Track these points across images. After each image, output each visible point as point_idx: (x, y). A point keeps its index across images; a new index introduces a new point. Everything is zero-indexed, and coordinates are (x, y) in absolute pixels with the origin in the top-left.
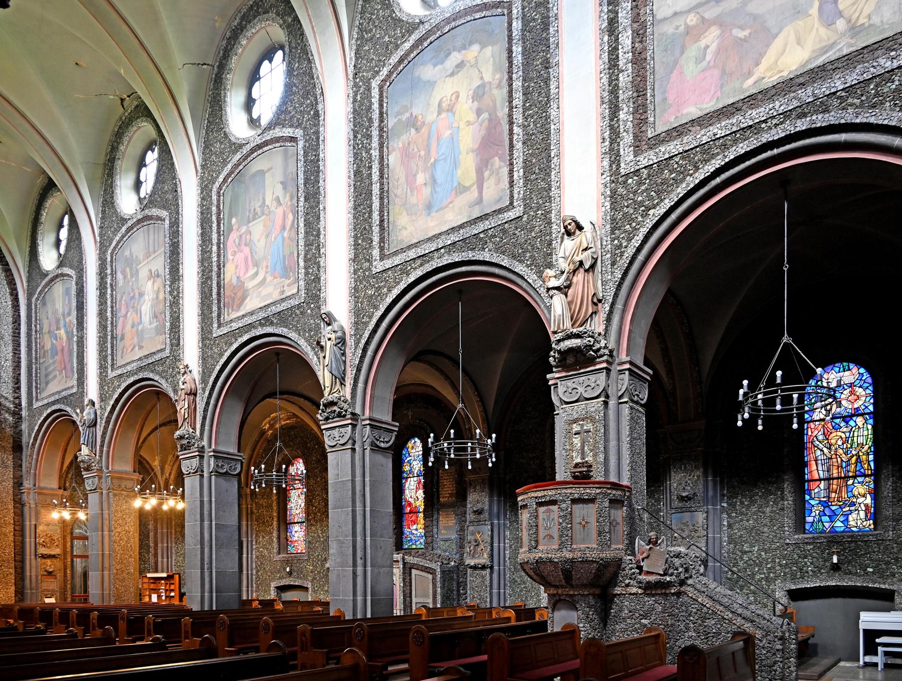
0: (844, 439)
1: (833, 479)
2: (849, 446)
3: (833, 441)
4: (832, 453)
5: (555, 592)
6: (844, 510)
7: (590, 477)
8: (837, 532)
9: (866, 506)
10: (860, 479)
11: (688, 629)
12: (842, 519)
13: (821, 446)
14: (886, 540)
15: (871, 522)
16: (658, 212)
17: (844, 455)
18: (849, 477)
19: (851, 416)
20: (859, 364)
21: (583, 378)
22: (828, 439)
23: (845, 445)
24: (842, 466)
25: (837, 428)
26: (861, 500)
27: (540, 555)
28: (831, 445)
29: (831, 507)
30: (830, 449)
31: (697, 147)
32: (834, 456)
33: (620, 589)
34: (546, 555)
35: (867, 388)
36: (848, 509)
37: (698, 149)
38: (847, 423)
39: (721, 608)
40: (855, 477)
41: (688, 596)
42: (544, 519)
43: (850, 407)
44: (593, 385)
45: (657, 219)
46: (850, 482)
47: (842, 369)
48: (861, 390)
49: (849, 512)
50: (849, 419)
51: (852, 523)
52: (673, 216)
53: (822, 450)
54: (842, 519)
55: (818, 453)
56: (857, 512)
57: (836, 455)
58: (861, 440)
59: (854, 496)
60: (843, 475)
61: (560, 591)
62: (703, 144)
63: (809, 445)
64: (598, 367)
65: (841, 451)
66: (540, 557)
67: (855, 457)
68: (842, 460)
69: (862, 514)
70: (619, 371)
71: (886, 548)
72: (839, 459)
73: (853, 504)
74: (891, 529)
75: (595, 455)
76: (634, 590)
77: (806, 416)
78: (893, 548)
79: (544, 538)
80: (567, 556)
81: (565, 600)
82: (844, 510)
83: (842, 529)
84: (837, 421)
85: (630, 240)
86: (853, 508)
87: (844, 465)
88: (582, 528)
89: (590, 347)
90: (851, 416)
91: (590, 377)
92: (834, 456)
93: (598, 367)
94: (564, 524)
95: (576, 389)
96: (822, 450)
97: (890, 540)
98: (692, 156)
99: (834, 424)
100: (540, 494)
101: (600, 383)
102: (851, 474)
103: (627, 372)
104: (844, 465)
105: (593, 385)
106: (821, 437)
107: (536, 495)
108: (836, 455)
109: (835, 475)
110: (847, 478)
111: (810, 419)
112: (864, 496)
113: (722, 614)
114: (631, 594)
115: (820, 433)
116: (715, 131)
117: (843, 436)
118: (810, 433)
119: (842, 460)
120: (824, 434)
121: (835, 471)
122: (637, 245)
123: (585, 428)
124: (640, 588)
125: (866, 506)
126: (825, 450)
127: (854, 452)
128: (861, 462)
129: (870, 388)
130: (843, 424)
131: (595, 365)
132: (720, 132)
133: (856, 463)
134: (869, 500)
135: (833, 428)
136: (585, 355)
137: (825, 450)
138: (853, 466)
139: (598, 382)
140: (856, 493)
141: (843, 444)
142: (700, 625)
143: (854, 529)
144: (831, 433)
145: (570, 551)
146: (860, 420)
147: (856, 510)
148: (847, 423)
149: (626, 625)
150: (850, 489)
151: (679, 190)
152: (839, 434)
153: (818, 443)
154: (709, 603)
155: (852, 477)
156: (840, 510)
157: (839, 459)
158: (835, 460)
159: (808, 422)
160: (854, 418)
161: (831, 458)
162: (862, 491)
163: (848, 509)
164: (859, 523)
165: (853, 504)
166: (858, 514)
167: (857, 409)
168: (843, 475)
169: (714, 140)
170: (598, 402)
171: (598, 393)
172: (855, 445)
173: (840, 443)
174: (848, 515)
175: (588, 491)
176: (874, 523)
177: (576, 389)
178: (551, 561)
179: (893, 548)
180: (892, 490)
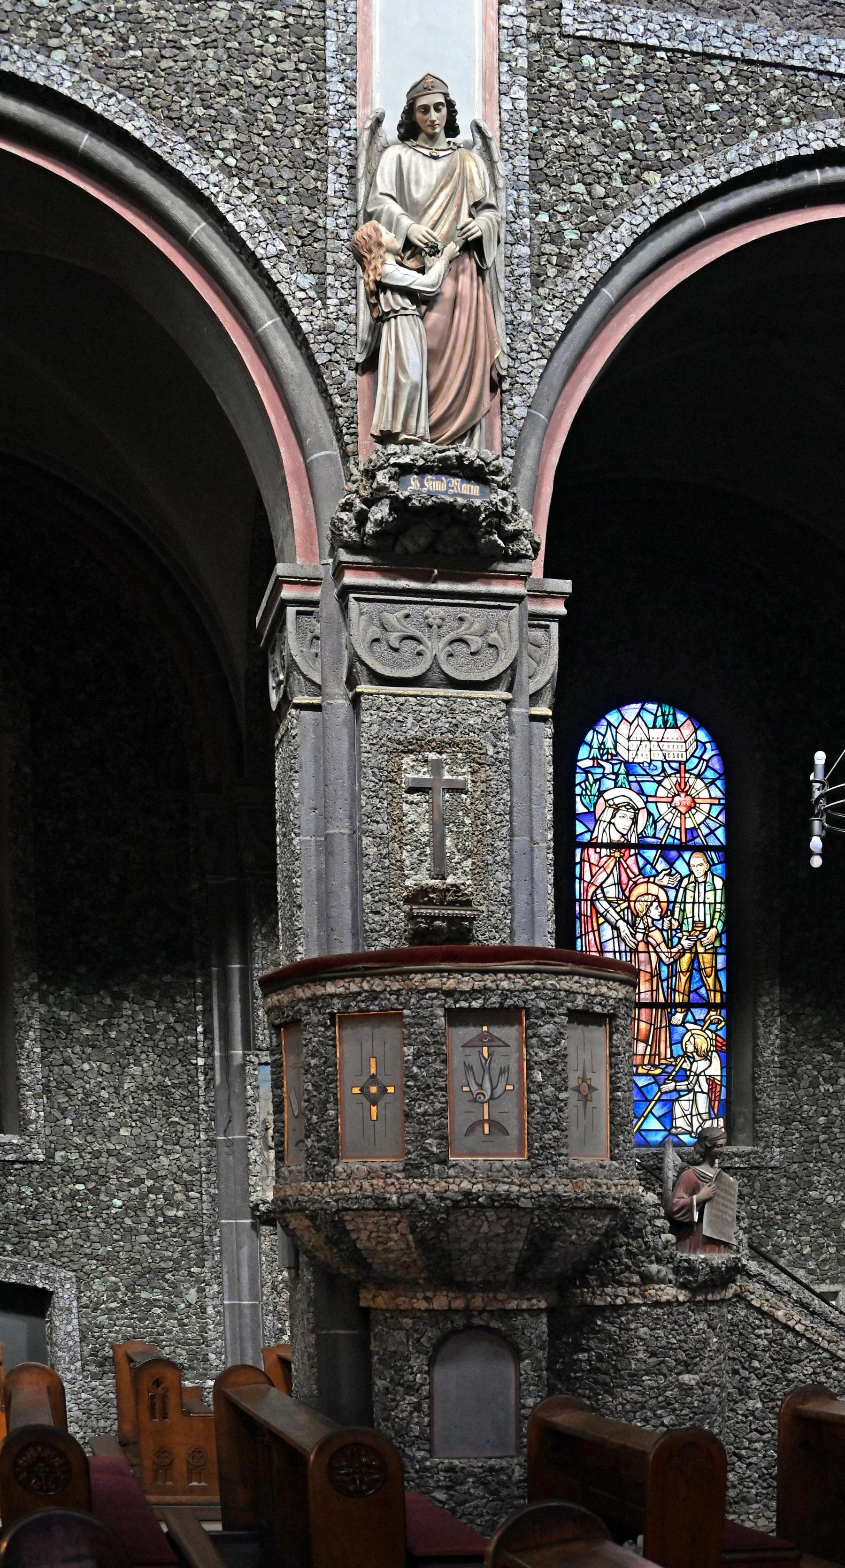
0: (664, 905)
1: (641, 1005)
2: (675, 924)
3: (640, 907)
4: (639, 936)
5: (459, 1304)
6: (665, 1088)
7: (465, 935)
8: (648, 1144)
9: (710, 1080)
10: (700, 1014)
11: (744, 1392)
12: (659, 1111)
13: (613, 915)
14: (766, 1168)
15: (721, 1121)
16: (676, 188)
17: (663, 947)
18: (675, 1005)
19: (681, 848)
20: (699, 720)
21: (441, 611)
22: (628, 899)
23: (666, 920)
24: (659, 975)
25: (646, 875)
26: (701, 1065)
27: (466, 1185)
28: (635, 915)
29: (636, 1079)
30: (633, 925)
31: (777, 65)
32: (642, 947)
33: (623, 1291)
34: (490, 1186)
35: (713, 782)
36: (672, 1085)
37: (778, 73)
38: (671, 864)
39: (828, 1332)
40: (687, 1006)
41: (749, 1305)
42: (469, 1068)
43: (677, 823)
44: (476, 643)
45: (671, 205)
46: (678, 1018)
47: (660, 721)
48: (699, 784)
49: (675, 1095)
50: (674, 854)
51: (681, 1123)
52: (703, 217)
53: (615, 927)
54: (659, 1111)
55: (607, 932)
56: (691, 1096)
57: (648, 943)
58: (701, 913)
59: (685, 1054)
60: (662, 999)
61: (478, 1302)
62: (793, 68)
63: (585, 908)
64: (497, 588)
65: (656, 935)
66: (467, 1194)
67: (688, 956)
68: (660, 959)
69: (702, 1102)
70: (533, 616)
71: (766, 1188)
72: (654, 956)
73: (684, 1075)
74: (777, 1142)
75: (481, 872)
76: (669, 1293)
77: (580, 828)
78: (779, 1187)
79: (471, 1130)
80: (560, 1189)
81: (487, 1328)
82: (665, 1088)
83: (659, 1137)
84: (650, 854)
85: (589, 231)
86: (682, 1086)
87: (664, 974)
88: (580, 1104)
89: (498, 517)
90: (681, 848)
91: (465, 612)
92: (642, 947)
93: (497, 588)
94: (549, 1090)
95: (419, 641)
96: (615, 927)
97: (773, 1168)
98: (763, 81)
99: (641, 862)
100: (467, 983)
101: (499, 643)
102: (678, 998)
103: (554, 627)
104: (664, 969)
105: (476, 643)
106: (611, 892)
107: (451, 984)
108: (648, 943)
109: (645, 997)
110: (669, 1006)
111: (587, 837)
112: (706, 1057)
113: (833, 1347)
114: (657, 1304)
115: (611, 881)
116: (826, 51)
117: (663, 897)
118: (587, 877)
119: (660, 959)
120: (619, 883)
121: (644, 987)
122: (615, 256)
123: (447, 776)
124: (682, 1286)
125: (710, 1080)
126: (622, 925)
127: (686, 943)
128: (700, 970)
129: (718, 783)
130: (661, 865)
131: (489, 578)
132: (834, 59)
133: (690, 970)
134: (715, 1069)
135: (640, 870)
136: (474, 539)
137: (622, 925)
138: (684, 979)
139: (493, 637)
140: (690, 1048)
141: (662, 917)
142: (777, 1380)
143: (685, 1138)
144: (636, 884)
145: (567, 1176)
146: (698, 861)
147: (689, 1091)
148: (671, 864)
149: (643, 1394)
150: (676, 1037)
151: (731, 156)
152: (654, 889)
153: (606, 905)
154: (800, 1322)
155: (681, 1005)
156: (655, 1088)
157: (654, 956)
158: (643, 957)
159: (585, 846)
160: (686, 855)
161: (635, 951)
162: (702, 1044)
163: (671, 1086)
164: (696, 1125)
165: (684, 1075)
166: (694, 1100)
167: (693, 832)
168: (662, 999)
169: (820, 73)
170: (492, 702)
171: (494, 673)
172: (688, 926)
173: (655, 913)
174: (673, 1101)
175: (604, 990)
176: (727, 1125)
177: (419, 641)
178: (381, 1205)
179: (779, 1187)
180: (781, 1047)
